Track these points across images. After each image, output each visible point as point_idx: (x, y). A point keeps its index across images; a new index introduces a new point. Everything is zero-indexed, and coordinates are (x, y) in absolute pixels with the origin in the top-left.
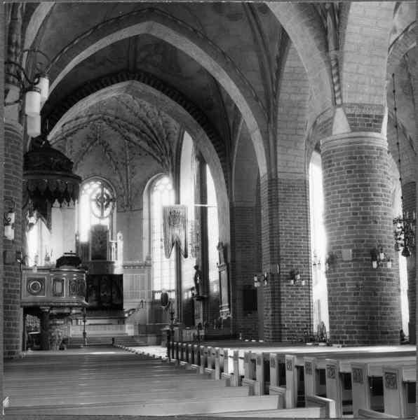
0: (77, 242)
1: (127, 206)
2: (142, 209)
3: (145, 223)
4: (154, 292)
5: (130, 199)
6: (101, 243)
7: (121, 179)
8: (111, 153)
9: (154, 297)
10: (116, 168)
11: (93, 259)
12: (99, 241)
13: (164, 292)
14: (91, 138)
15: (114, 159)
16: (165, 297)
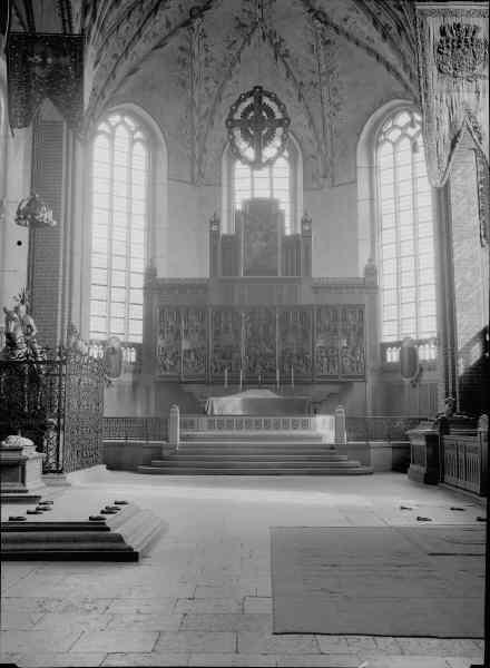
0: (214, 235)
1: (325, 177)
2: (355, 182)
3: (363, 208)
4: (384, 347)
5: (332, 163)
6: (266, 238)
7: (311, 122)
8: (287, 60)
9: (384, 357)
10: (300, 96)
11: (246, 273)
12: (260, 234)
13: (405, 345)
14: (244, 26)
15: (297, 76)
16: (410, 353)
